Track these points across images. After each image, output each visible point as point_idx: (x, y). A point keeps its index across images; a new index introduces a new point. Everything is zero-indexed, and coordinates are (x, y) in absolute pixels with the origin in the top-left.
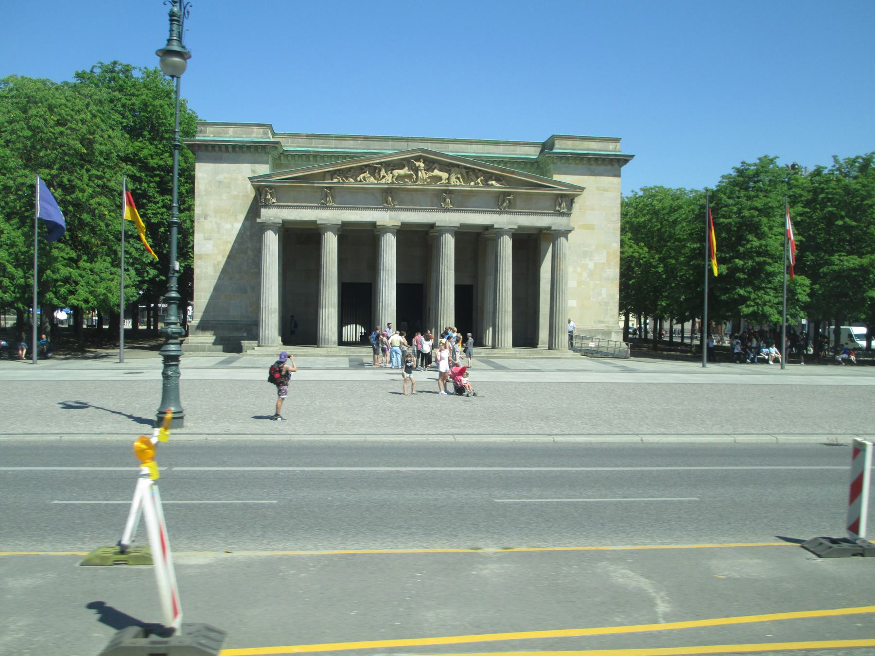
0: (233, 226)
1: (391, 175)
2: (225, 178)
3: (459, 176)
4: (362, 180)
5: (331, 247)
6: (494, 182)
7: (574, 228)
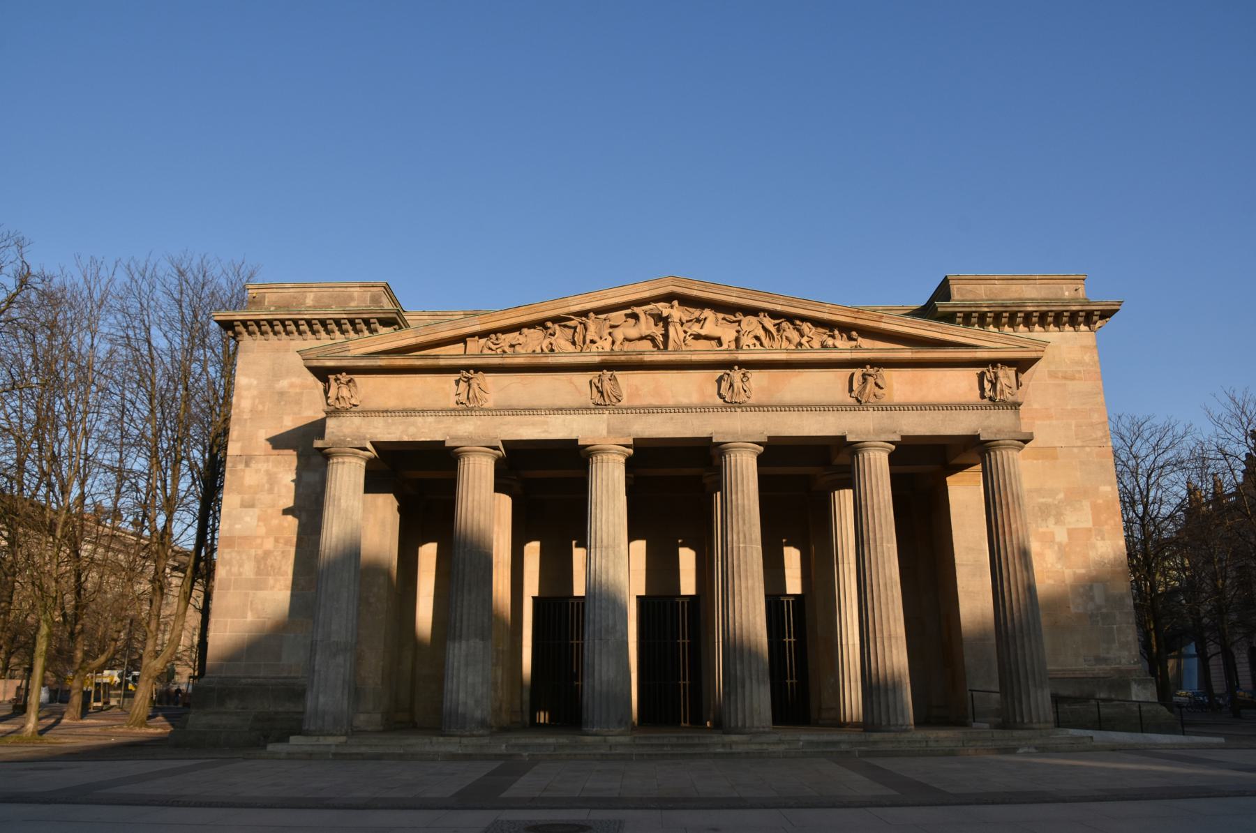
1: (610, 339)
2: (292, 385)
3: (761, 333)
4: (546, 350)
5: (477, 497)
6: (839, 343)
7: (1032, 434)
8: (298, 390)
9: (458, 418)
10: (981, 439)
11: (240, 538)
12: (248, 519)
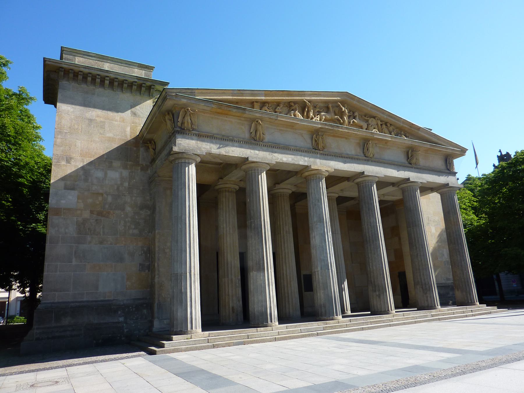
0: (106, 174)
2: (98, 116)
8: (102, 119)
9: (251, 147)
10: (450, 185)
11: (64, 209)
12: (70, 197)
